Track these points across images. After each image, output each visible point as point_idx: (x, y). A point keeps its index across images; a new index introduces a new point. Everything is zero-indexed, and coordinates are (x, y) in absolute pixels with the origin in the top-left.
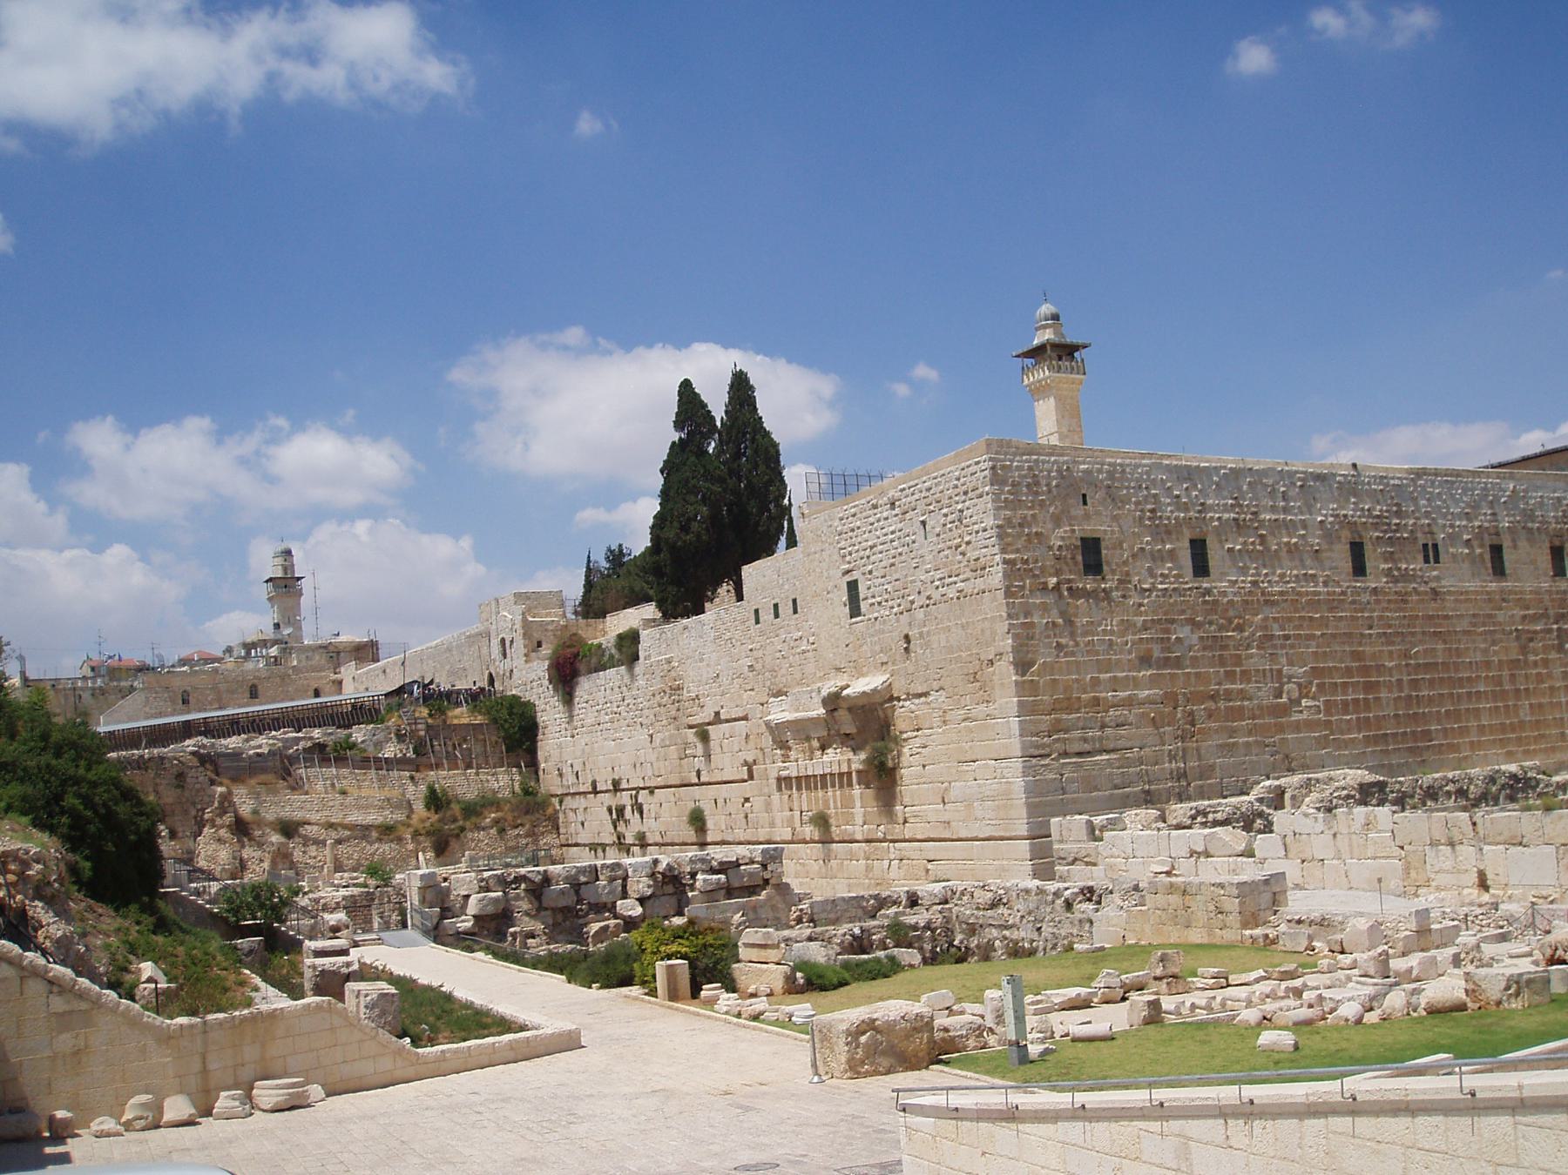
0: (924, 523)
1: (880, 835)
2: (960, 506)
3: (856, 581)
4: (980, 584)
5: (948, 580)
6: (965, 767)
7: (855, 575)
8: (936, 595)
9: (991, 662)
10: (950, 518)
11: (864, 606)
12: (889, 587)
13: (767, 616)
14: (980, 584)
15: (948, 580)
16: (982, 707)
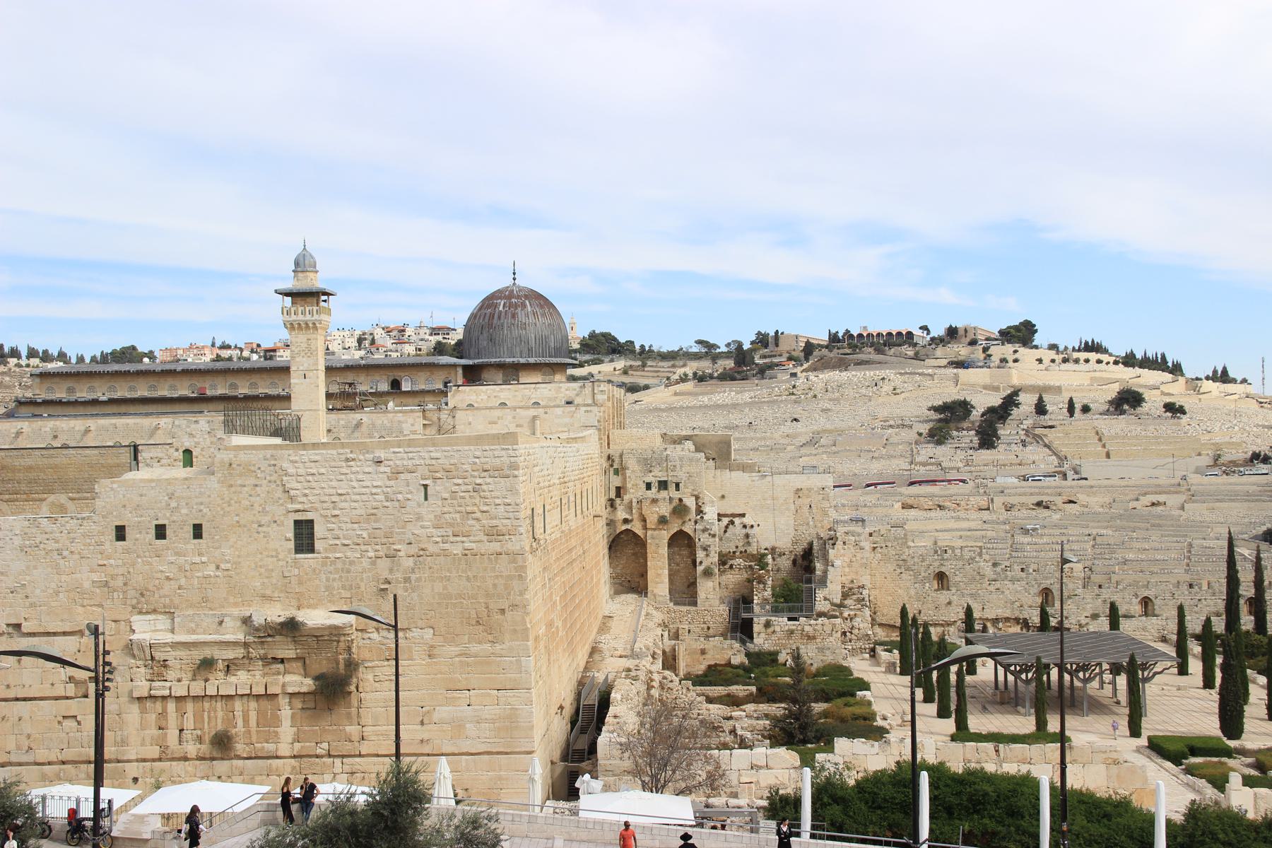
0: (426, 486)
1: (319, 751)
2: (478, 481)
3: (312, 521)
4: (496, 547)
5: (452, 539)
6: (457, 694)
7: (309, 516)
8: (432, 548)
9: (503, 611)
10: (463, 488)
11: (318, 545)
12: (365, 535)
13: (141, 536)
14: (496, 547)
15: (452, 539)
16: (487, 646)
